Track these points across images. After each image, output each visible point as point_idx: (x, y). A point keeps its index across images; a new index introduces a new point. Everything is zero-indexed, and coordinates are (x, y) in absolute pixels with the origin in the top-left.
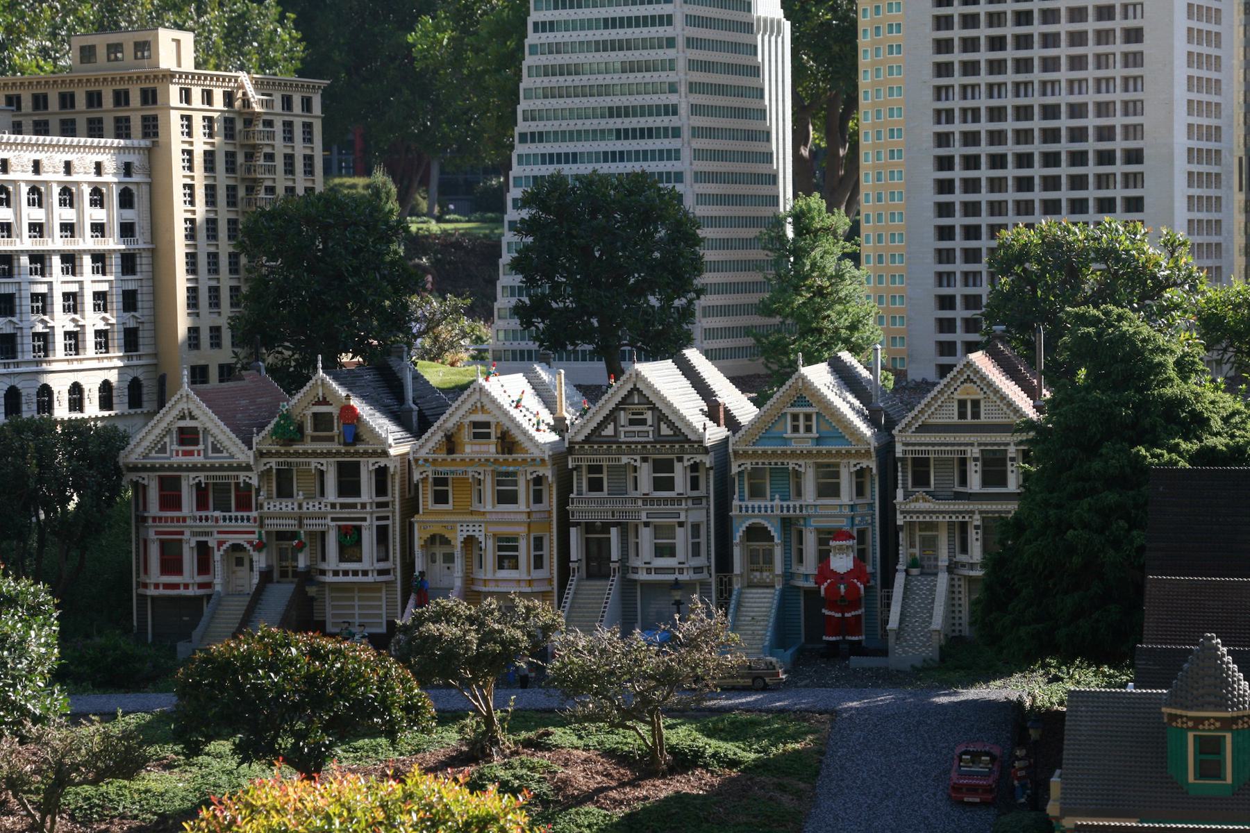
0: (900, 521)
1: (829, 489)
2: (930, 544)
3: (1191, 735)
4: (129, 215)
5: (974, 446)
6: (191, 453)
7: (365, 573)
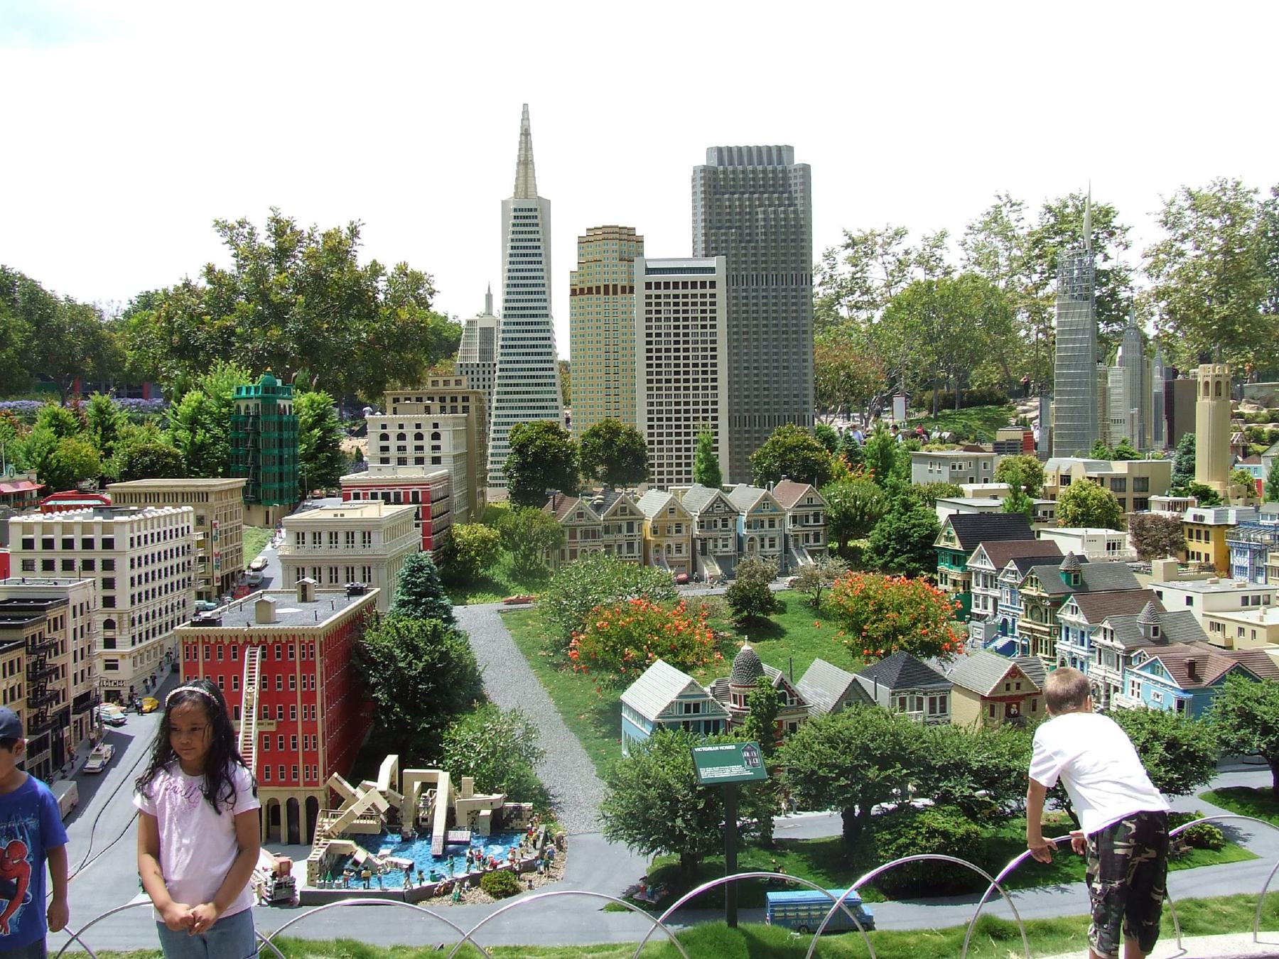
2: (796, 540)
5: (811, 511)
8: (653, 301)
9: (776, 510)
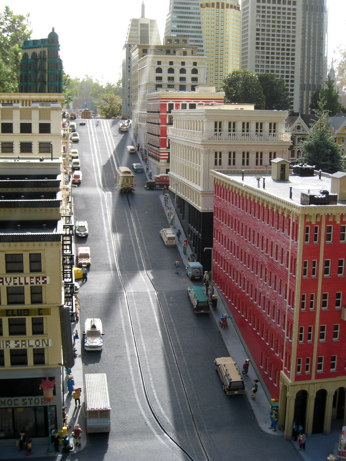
6: (299, 131)
8: (261, 9)
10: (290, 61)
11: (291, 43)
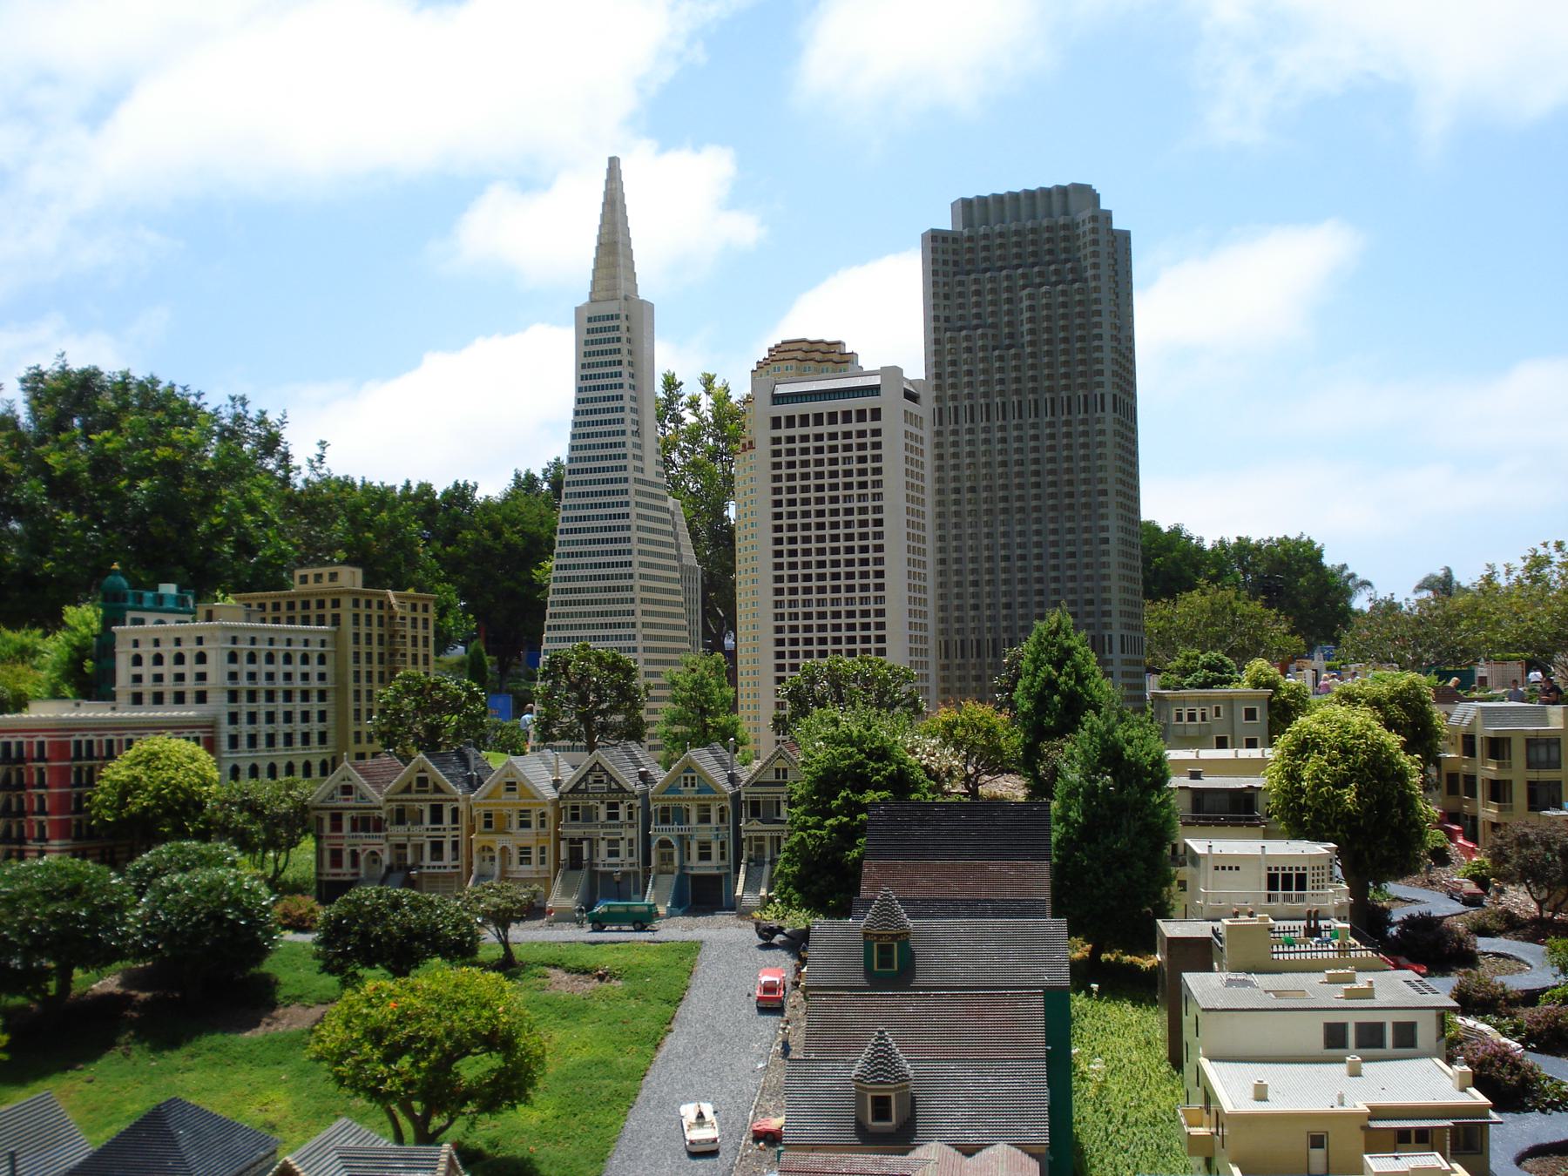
0: (743, 836)
1: (705, 819)
3: (875, 945)
4: (323, 668)
6: (347, 800)
7: (445, 867)
8: (784, 446)
9: (711, 791)
10: (872, 581)
11: (871, 529)
